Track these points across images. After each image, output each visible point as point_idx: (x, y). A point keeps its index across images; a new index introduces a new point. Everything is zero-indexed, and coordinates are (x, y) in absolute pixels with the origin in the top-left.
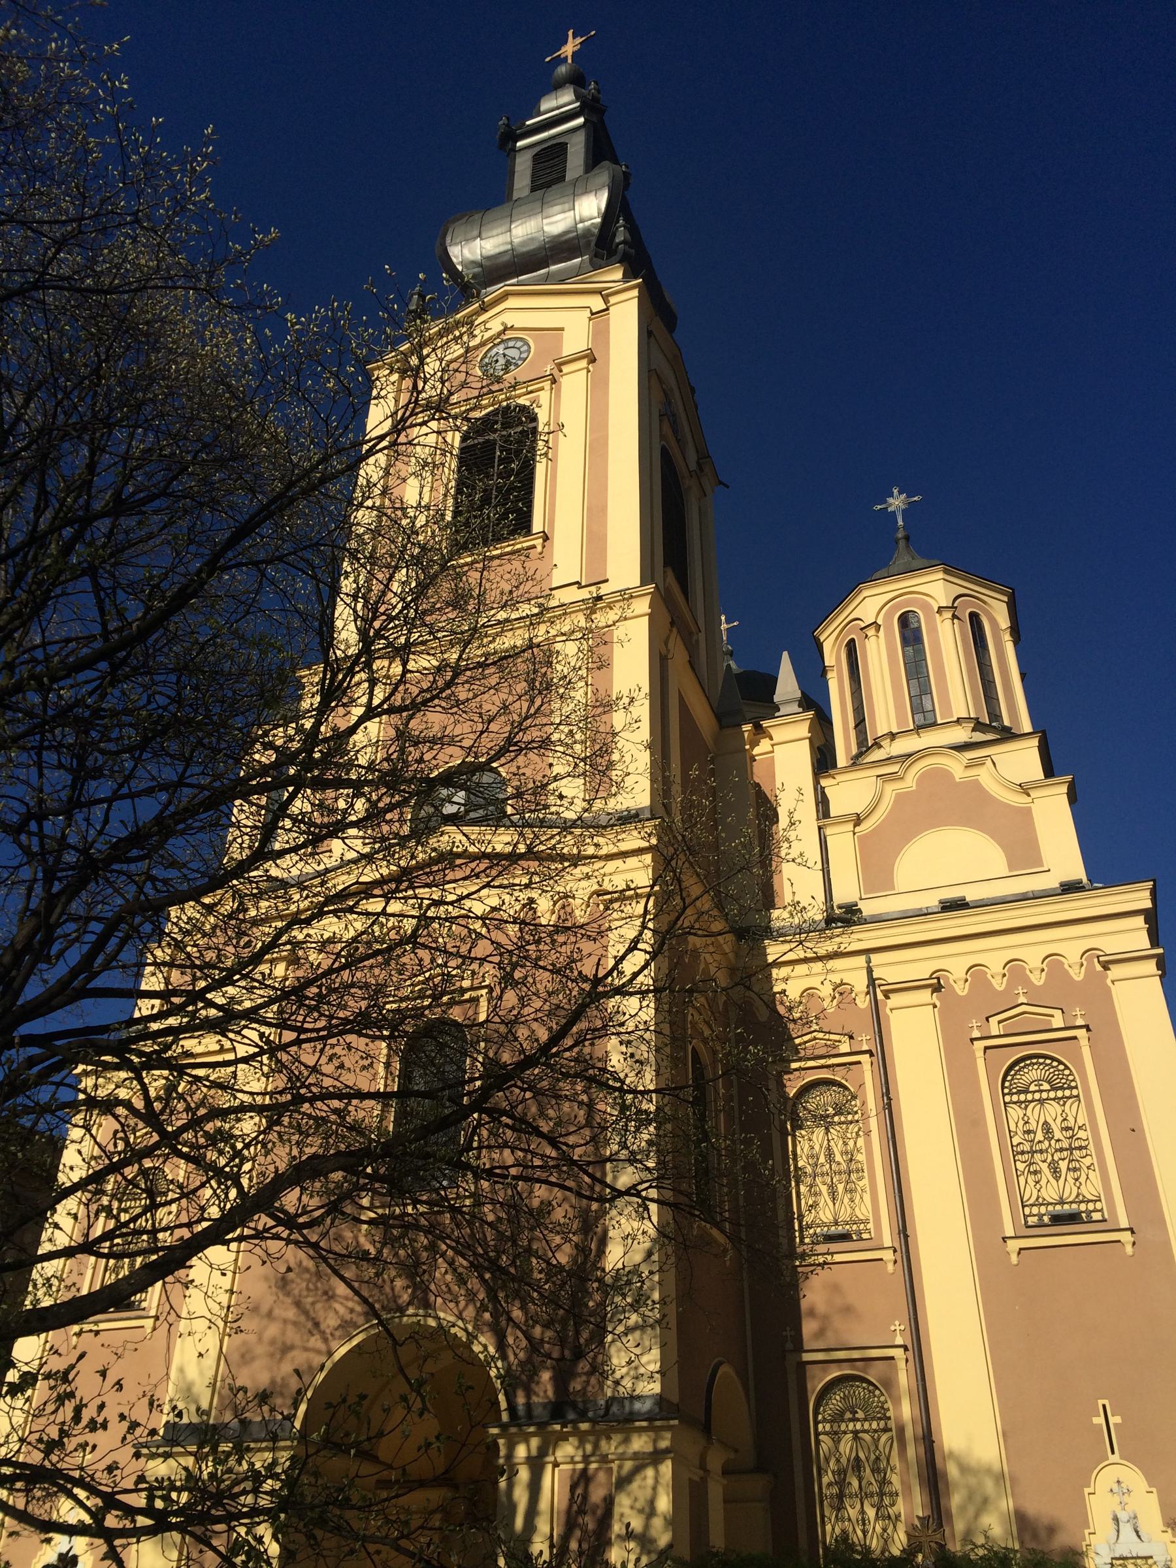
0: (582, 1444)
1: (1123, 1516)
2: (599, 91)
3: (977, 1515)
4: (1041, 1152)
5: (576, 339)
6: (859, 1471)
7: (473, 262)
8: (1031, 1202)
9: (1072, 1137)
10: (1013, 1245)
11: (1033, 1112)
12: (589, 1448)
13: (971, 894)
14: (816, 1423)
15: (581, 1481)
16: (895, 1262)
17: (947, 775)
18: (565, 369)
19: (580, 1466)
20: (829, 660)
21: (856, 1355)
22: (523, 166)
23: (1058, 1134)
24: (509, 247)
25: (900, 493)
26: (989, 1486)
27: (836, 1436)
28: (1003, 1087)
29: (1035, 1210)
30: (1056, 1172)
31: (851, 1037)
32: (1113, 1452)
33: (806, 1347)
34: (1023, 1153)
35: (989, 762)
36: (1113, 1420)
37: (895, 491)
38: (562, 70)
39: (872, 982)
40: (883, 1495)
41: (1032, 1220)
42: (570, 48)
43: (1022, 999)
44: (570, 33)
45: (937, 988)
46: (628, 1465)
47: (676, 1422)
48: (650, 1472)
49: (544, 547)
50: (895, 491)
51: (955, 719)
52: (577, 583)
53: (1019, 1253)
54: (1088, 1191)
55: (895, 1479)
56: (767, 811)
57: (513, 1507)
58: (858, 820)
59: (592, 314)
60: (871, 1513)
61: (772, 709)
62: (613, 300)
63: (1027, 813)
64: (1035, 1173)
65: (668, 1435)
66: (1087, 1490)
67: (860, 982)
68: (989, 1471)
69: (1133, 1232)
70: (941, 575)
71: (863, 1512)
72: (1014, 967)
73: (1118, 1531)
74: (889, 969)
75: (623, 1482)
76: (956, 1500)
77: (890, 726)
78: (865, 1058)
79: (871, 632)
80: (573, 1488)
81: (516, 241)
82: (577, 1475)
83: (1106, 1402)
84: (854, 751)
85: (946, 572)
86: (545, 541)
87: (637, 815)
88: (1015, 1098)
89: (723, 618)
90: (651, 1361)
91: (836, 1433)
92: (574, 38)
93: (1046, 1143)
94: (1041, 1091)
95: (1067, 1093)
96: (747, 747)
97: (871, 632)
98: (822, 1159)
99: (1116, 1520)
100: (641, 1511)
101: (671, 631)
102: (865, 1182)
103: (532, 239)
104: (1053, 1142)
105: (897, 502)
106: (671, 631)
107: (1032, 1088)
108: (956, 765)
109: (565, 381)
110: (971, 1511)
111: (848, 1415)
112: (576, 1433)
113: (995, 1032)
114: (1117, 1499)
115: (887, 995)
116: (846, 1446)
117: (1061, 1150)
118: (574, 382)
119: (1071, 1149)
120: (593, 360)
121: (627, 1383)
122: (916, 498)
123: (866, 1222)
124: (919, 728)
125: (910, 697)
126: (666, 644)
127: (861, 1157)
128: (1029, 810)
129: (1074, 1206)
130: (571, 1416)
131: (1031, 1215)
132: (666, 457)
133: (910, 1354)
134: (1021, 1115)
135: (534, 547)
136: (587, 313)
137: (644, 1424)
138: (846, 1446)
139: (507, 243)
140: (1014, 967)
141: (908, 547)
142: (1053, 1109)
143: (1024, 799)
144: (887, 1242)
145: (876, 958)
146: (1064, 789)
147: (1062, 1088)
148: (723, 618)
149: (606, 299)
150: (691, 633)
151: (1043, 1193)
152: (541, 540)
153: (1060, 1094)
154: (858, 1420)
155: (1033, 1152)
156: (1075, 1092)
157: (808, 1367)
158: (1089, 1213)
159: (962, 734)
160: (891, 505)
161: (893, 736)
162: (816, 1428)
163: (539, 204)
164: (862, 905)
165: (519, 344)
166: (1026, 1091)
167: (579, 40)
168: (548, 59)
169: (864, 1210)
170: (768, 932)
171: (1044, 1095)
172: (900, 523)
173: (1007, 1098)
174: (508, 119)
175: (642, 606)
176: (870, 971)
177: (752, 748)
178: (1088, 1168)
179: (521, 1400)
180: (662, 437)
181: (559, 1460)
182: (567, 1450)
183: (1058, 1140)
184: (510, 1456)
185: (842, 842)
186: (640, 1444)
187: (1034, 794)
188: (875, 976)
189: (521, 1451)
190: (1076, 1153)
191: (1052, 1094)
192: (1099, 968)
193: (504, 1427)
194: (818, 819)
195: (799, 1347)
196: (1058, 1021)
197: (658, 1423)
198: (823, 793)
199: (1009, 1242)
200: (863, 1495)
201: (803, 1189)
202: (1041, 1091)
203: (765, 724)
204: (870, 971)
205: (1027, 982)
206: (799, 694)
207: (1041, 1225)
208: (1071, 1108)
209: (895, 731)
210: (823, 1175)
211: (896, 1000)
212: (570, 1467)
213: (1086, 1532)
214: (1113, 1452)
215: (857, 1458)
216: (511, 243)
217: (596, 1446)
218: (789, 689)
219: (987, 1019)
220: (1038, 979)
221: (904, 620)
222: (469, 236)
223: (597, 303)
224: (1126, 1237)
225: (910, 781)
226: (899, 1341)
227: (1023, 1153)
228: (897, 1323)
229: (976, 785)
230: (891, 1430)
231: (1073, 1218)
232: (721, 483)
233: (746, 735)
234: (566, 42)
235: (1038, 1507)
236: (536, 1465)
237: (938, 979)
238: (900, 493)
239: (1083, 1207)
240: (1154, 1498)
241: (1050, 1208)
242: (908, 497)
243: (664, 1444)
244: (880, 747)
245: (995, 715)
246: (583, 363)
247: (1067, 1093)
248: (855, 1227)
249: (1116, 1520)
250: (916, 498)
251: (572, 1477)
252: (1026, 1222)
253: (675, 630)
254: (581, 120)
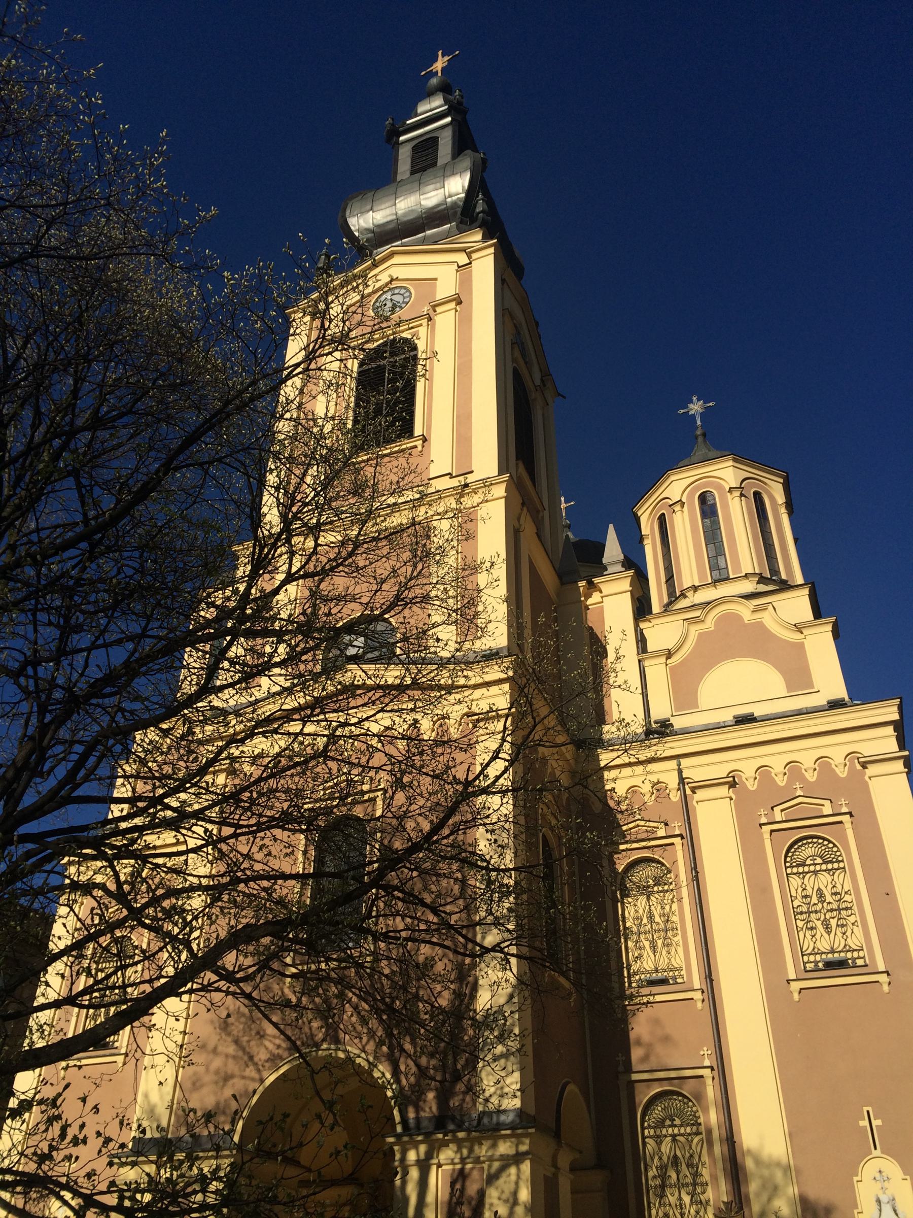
0: (459, 1150)
1: (884, 1199)
2: (462, 97)
3: (770, 1200)
4: (816, 912)
5: (446, 286)
6: (677, 1166)
7: (368, 230)
8: (808, 952)
9: (839, 900)
10: (795, 986)
11: (809, 881)
12: (465, 1152)
13: (759, 711)
14: (643, 1129)
15: (459, 1178)
16: (703, 1001)
17: (739, 618)
18: (439, 309)
19: (459, 1166)
20: (645, 530)
21: (673, 1074)
22: (405, 155)
23: (829, 898)
24: (394, 217)
25: (698, 400)
26: (779, 1176)
27: (659, 1139)
28: (785, 862)
29: (812, 958)
31: (666, 824)
32: (875, 1148)
33: (634, 1069)
34: (801, 913)
35: (770, 607)
36: (875, 1123)
37: (695, 399)
38: (434, 81)
39: (682, 780)
40: (696, 1184)
41: (810, 966)
42: (440, 64)
43: (799, 793)
44: (440, 53)
45: (733, 785)
46: (496, 1165)
47: (532, 1130)
48: (513, 1170)
49: (423, 447)
50: (695, 399)
51: (743, 574)
52: (449, 474)
53: (800, 992)
54: (853, 943)
55: (706, 1173)
56: (598, 648)
57: (406, 1200)
58: (669, 654)
59: (459, 267)
60: (687, 1199)
61: (601, 569)
62: (474, 256)
63: (800, 647)
64: (812, 928)
65: (527, 1141)
66: (855, 1179)
67: (672, 780)
68: (778, 1164)
69: (889, 975)
70: (731, 463)
71: (680, 1199)
73: (880, 1210)
74: (695, 770)
75: (492, 1179)
76: (753, 1187)
77: (693, 580)
78: (677, 841)
79: (677, 508)
80: (453, 1184)
81: (400, 212)
82: (455, 1175)
83: (870, 1109)
84: (666, 600)
85: (735, 460)
86: (424, 442)
87: (497, 653)
88: (795, 870)
89: (563, 499)
90: (513, 1081)
91: (658, 1137)
92: (443, 56)
93: (820, 905)
94: (815, 864)
95: (836, 865)
96: (583, 599)
97: (677, 508)
98: (645, 921)
99: (879, 1201)
100: (506, 1201)
101: (522, 510)
102: (679, 938)
103: (412, 211)
104: (825, 904)
105: (696, 407)
106: (522, 510)
107: (808, 862)
108: (745, 610)
109: (438, 319)
110: (765, 1197)
111: (668, 1122)
112: (456, 1140)
113: (778, 819)
114: (879, 1185)
115: (693, 790)
116: (666, 1147)
117: (832, 910)
118: (446, 320)
119: (839, 910)
120: (459, 302)
121: (495, 1100)
122: (711, 404)
123: (680, 969)
124: (715, 582)
125: (709, 558)
126: (519, 519)
127: (675, 918)
128: (803, 644)
129: (842, 954)
130: (451, 1127)
131: (809, 962)
132: (517, 376)
133: (716, 1073)
134: (800, 884)
135: (416, 447)
136: (455, 267)
137: (508, 1132)
138: (666, 1147)
139: (392, 214)
141: (705, 441)
142: (824, 880)
143: (798, 636)
144: (697, 985)
145: (685, 762)
146: (829, 628)
147: (831, 862)
148: (563, 499)
149: (469, 255)
150: (538, 511)
151: (818, 944)
152: (421, 442)
153: (830, 866)
154: (675, 1126)
155: (809, 913)
156: (841, 865)
157: (637, 1085)
158: (854, 959)
159: (749, 586)
160: (691, 410)
161: (695, 588)
162: (643, 1133)
163: (416, 184)
164: (673, 721)
165: (403, 291)
166: (804, 865)
167: (446, 58)
168: (423, 73)
169: (678, 960)
170: (600, 743)
171: (818, 868)
172: (699, 423)
173: (789, 870)
174: (393, 119)
175: (500, 491)
176: (680, 772)
177: (586, 599)
178: (853, 924)
179: (411, 1115)
180: (514, 360)
181: (442, 1162)
182: (447, 1154)
183: (829, 903)
184: (403, 1159)
185: (657, 671)
186: (505, 1148)
187: (805, 632)
188: (684, 776)
189: (412, 1156)
190: (844, 913)
191: (824, 867)
192: (859, 767)
193: (398, 1137)
194: (638, 654)
195: (629, 1069)
196: (827, 809)
197: (519, 1131)
198: (642, 633)
199: (792, 983)
200: (680, 1185)
201: (630, 944)
202: (815, 864)
203: (596, 580)
204: (680, 772)
205: (803, 779)
206: (622, 557)
207: (817, 970)
208: (839, 877)
209: (697, 584)
210: (645, 933)
211: (701, 794)
212: (450, 1167)
213: (856, 1211)
214: (875, 1148)
215: (675, 1156)
216: (396, 214)
217: (471, 1151)
218: (614, 553)
219: (772, 808)
220: (811, 777)
221: (703, 498)
222: (363, 210)
223: (462, 259)
224: (883, 978)
225: (710, 623)
226: (707, 1063)
227: (801, 913)
228: (705, 1049)
229: (761, 626)
230: (701, 1133)
231: (841, 964)
232: (559, 395)
233: (581, 589)
234: (436, 60)
235: (818, 1193)
236: (424, 1166)
237: (734, 777)
238: (698, 400)
239: (849, 955)
240: (908, 1183)
241: (824, 956)
242: (705, 403)
243: (524, 1148)
244: (686, 597)
245: (774, 571)
246: (452, 305)
247: (836, 865)
248: (671, 974)
249: (879, 1201)
250: (711, 404)
251: (452, 1175)
252: (805, 967)
253: (525, 509)
254: (449, 119)
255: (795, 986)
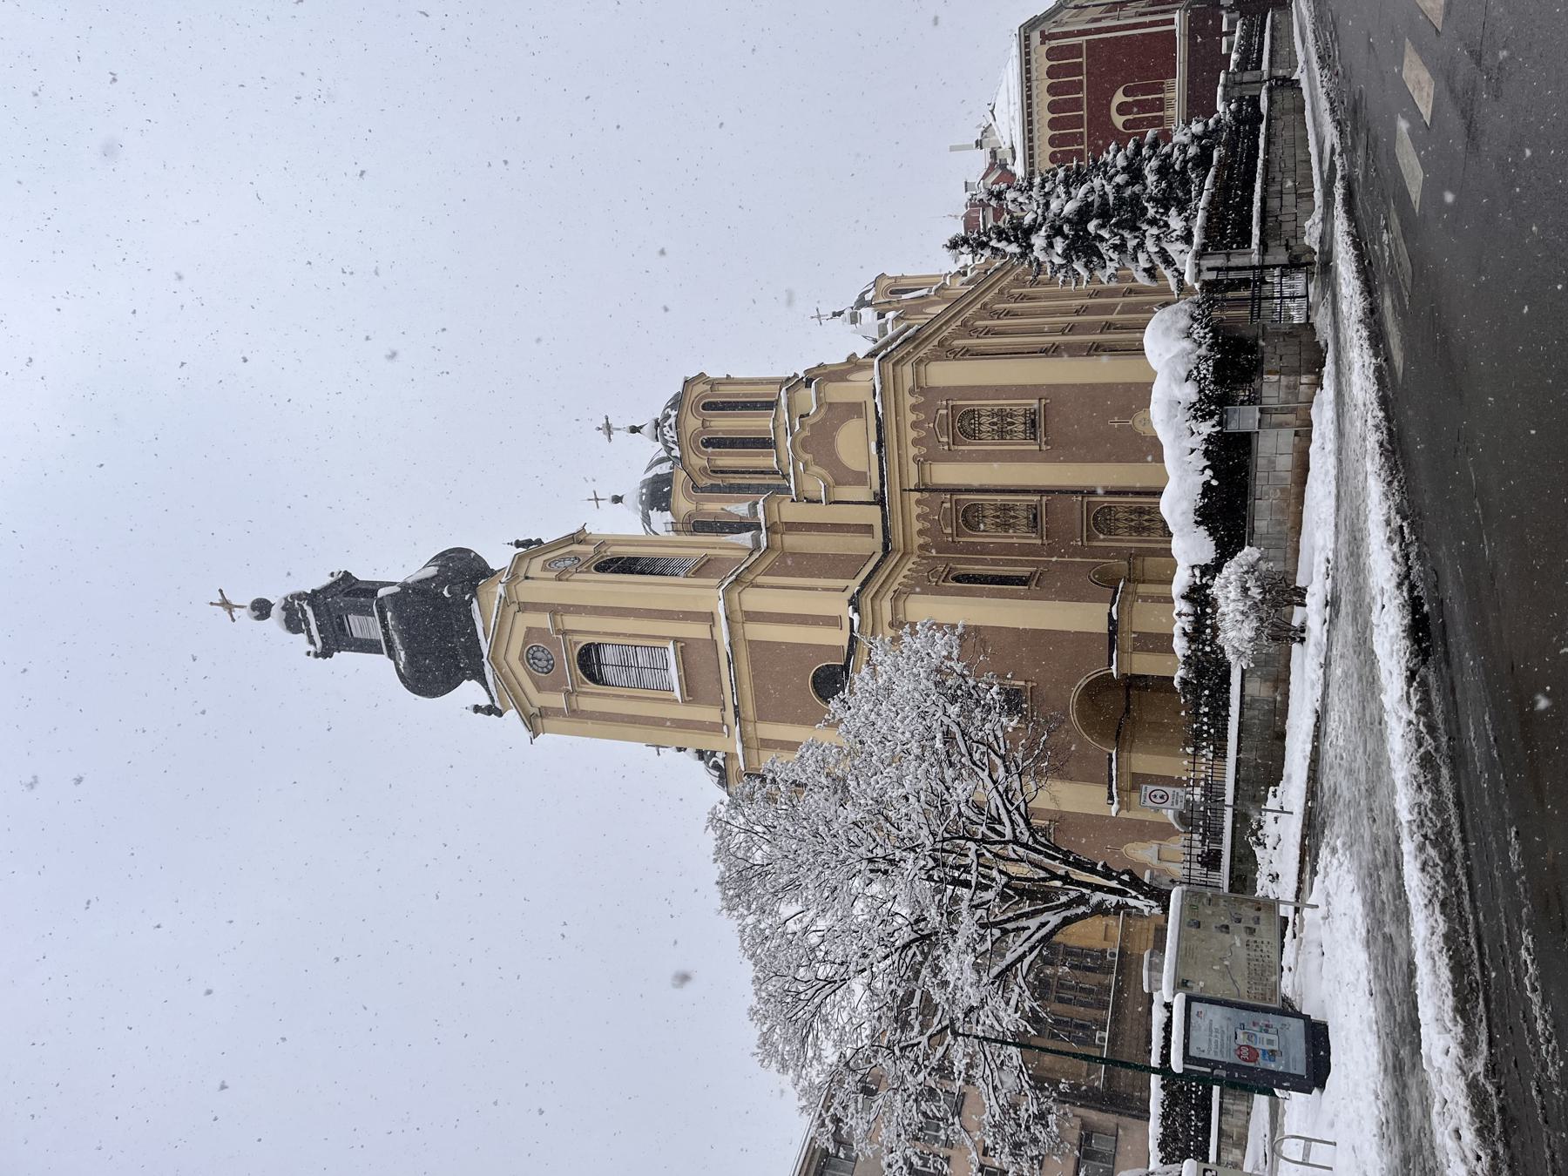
30: (1014, 424)
41: (1032, 436)
43: (931, 425)
67: (917, 495)
72: (915, 425)
74: (913, 481)
118: (571, 622)
140: (915, 425)
142: (983, 420)
176: (911, 490)
204: (911, 490)
207: (1034, 433)
224: (1043, 401)
255: (1044, 447)
